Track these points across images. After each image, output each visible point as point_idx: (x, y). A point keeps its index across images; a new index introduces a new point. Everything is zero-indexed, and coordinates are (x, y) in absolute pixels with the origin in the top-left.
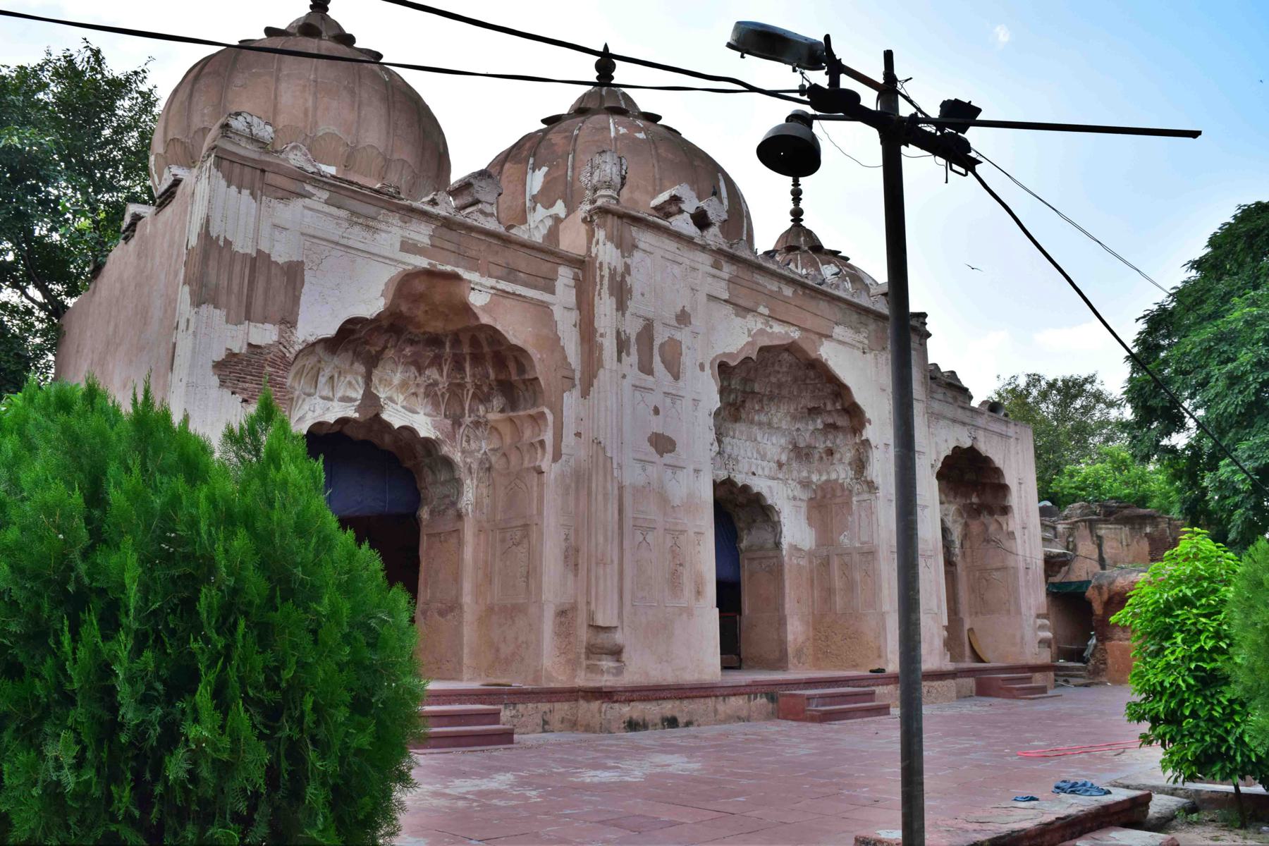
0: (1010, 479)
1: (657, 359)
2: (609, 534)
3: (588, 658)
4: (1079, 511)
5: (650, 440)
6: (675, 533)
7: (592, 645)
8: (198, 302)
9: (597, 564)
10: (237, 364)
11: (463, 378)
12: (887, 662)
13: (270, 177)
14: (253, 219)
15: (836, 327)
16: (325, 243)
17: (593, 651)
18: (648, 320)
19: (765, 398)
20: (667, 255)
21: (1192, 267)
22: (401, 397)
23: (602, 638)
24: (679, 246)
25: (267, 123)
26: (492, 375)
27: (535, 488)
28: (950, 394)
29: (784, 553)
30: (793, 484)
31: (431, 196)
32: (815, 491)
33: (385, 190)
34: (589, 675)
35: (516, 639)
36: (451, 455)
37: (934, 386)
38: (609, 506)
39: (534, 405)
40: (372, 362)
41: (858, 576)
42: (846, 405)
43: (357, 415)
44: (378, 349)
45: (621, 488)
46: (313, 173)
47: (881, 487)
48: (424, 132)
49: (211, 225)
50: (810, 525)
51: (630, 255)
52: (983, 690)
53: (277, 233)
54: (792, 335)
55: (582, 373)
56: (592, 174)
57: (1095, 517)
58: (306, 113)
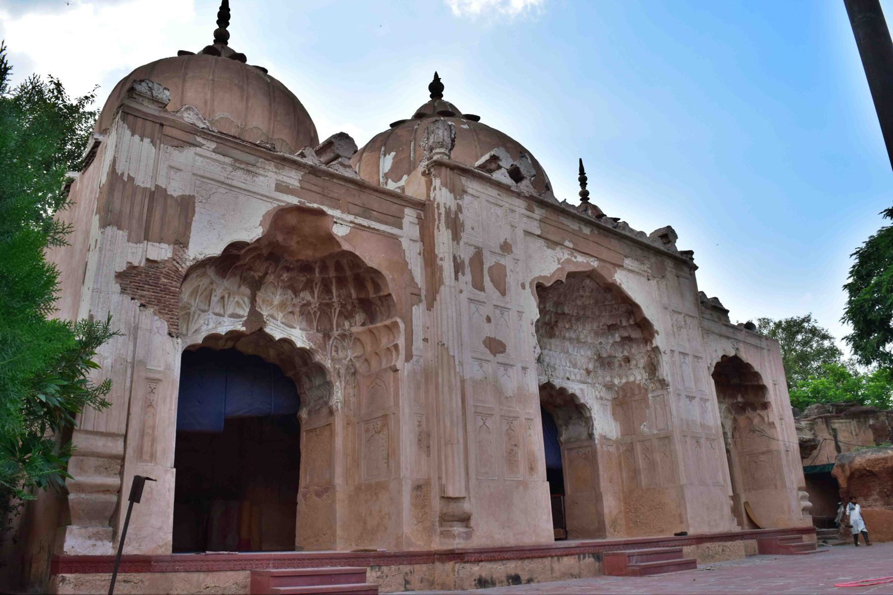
0: (767, 379)
1: (487, 278)
2: (455, 418)
3: (441, 525)
4: (816, 411)
5: (484, 343)
6: (510, 419)
7: (445, 514)
8: (104, 225)
9: (446, 445)
10: (136, 275)
11: (331, 299)
12: (688, 526)
13: (167, 130)
14: (152, 161)
15: (625, 259)
16: (213, 182)
17: (445, 519)
18: (478, 248)
19: (573, 319)
20: (491, 199)
21: (887, 215)
22: (280, 315)
23: (453, 508)
24: (499, 192)
25: (165, 89)
26: (354, 295)
27: (392, 384)
28: (715, 315)
29: (597, 441)
30: (599, 387)
31: (300, 151)
32: (617, 392)
33: (263, 145)
34: (442, 540)
35: (380, 511)
36: (323, 362)
37: (703, 308)
38: (454, 396)
39: (389, 317)
40: (256, 286)
41: (658, 457)
42: (638, 320)
43: (244, 329)
44: (261, 274)
45: (463, 381)
46: (203, 128)
47: (671, 384)
48: (298, 119)
49: (117, 164)
50: (615, 419)
51: (461, 198)
52: (764, 549)
53: (172, 173)
54: (592, 263)
55: (427, 291)
56: (428, 139)
57: (829, 414)
58: (206, 102)
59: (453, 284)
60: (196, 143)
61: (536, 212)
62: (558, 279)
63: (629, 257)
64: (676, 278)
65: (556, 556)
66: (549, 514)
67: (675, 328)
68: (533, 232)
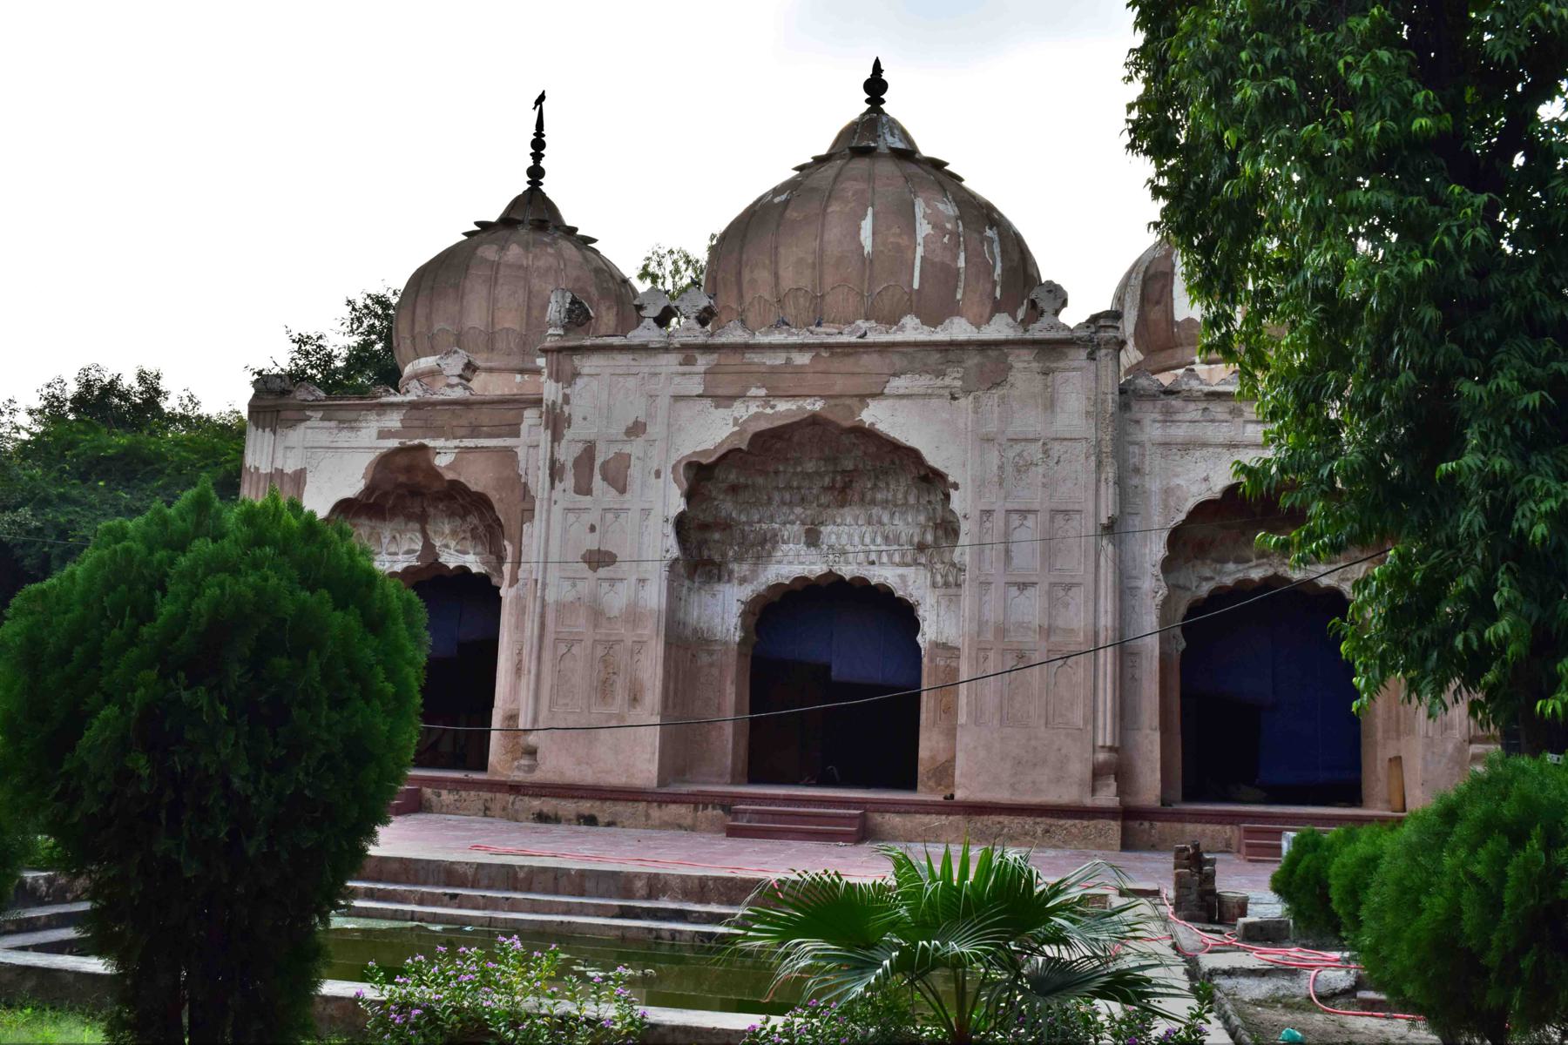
1: (597, 477)
20: (618, 371)
24: (636, 356)
45: (544, 605)
48: (530, 292)
54: (808, 408)
59: (546, 496)
60: (304, 417)
61: (699, 362)
62: (731, 447)
63: (905, 373)
64: (1039, 377)
65: (655, 801)
66: (654, 753)
67: (1009, 469)
68: (687, 393)
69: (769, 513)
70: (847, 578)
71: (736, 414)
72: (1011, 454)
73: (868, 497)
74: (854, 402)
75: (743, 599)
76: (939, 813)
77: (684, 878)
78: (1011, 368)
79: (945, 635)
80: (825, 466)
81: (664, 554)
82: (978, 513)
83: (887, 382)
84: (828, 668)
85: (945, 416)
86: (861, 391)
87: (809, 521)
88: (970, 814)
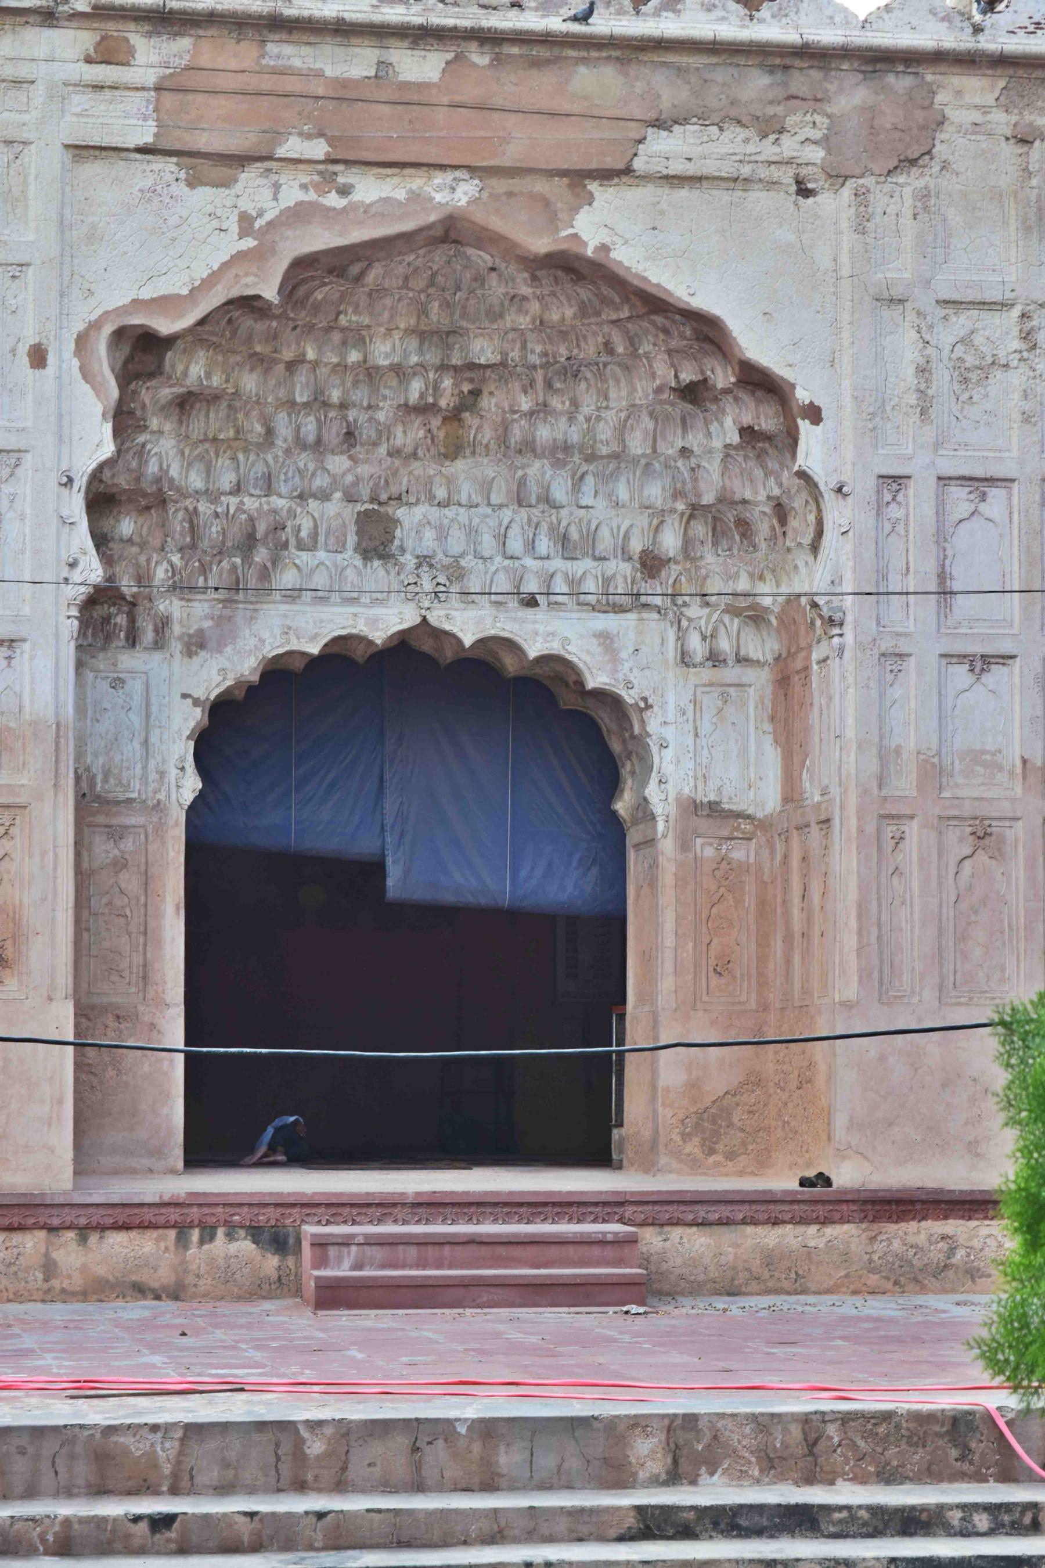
29: (661, 826)
47: (849, 619)
54: (438, 197)
61: (140, 58)
62: (235, 292)
64: (1010, 150)
66: (60, 1102)
67: (943, 378)
69: (260, 469)
70: (468, 641)
71: (247, 205)
72: (945, 337)
73: (517, 433)
74: (556, 189)
75: (200, 693)
76: (803, 1221)
77: (764, 1423)
78: (942, 122)
79: (713, 784)
80: (421, 352)
81: (65, 572)
82: (872, 482)
83: (641, 141)
84: (376, 869)
85: (785, 235)
86: (575, 162)
87: (365, 492)
88: (875, 1219)
